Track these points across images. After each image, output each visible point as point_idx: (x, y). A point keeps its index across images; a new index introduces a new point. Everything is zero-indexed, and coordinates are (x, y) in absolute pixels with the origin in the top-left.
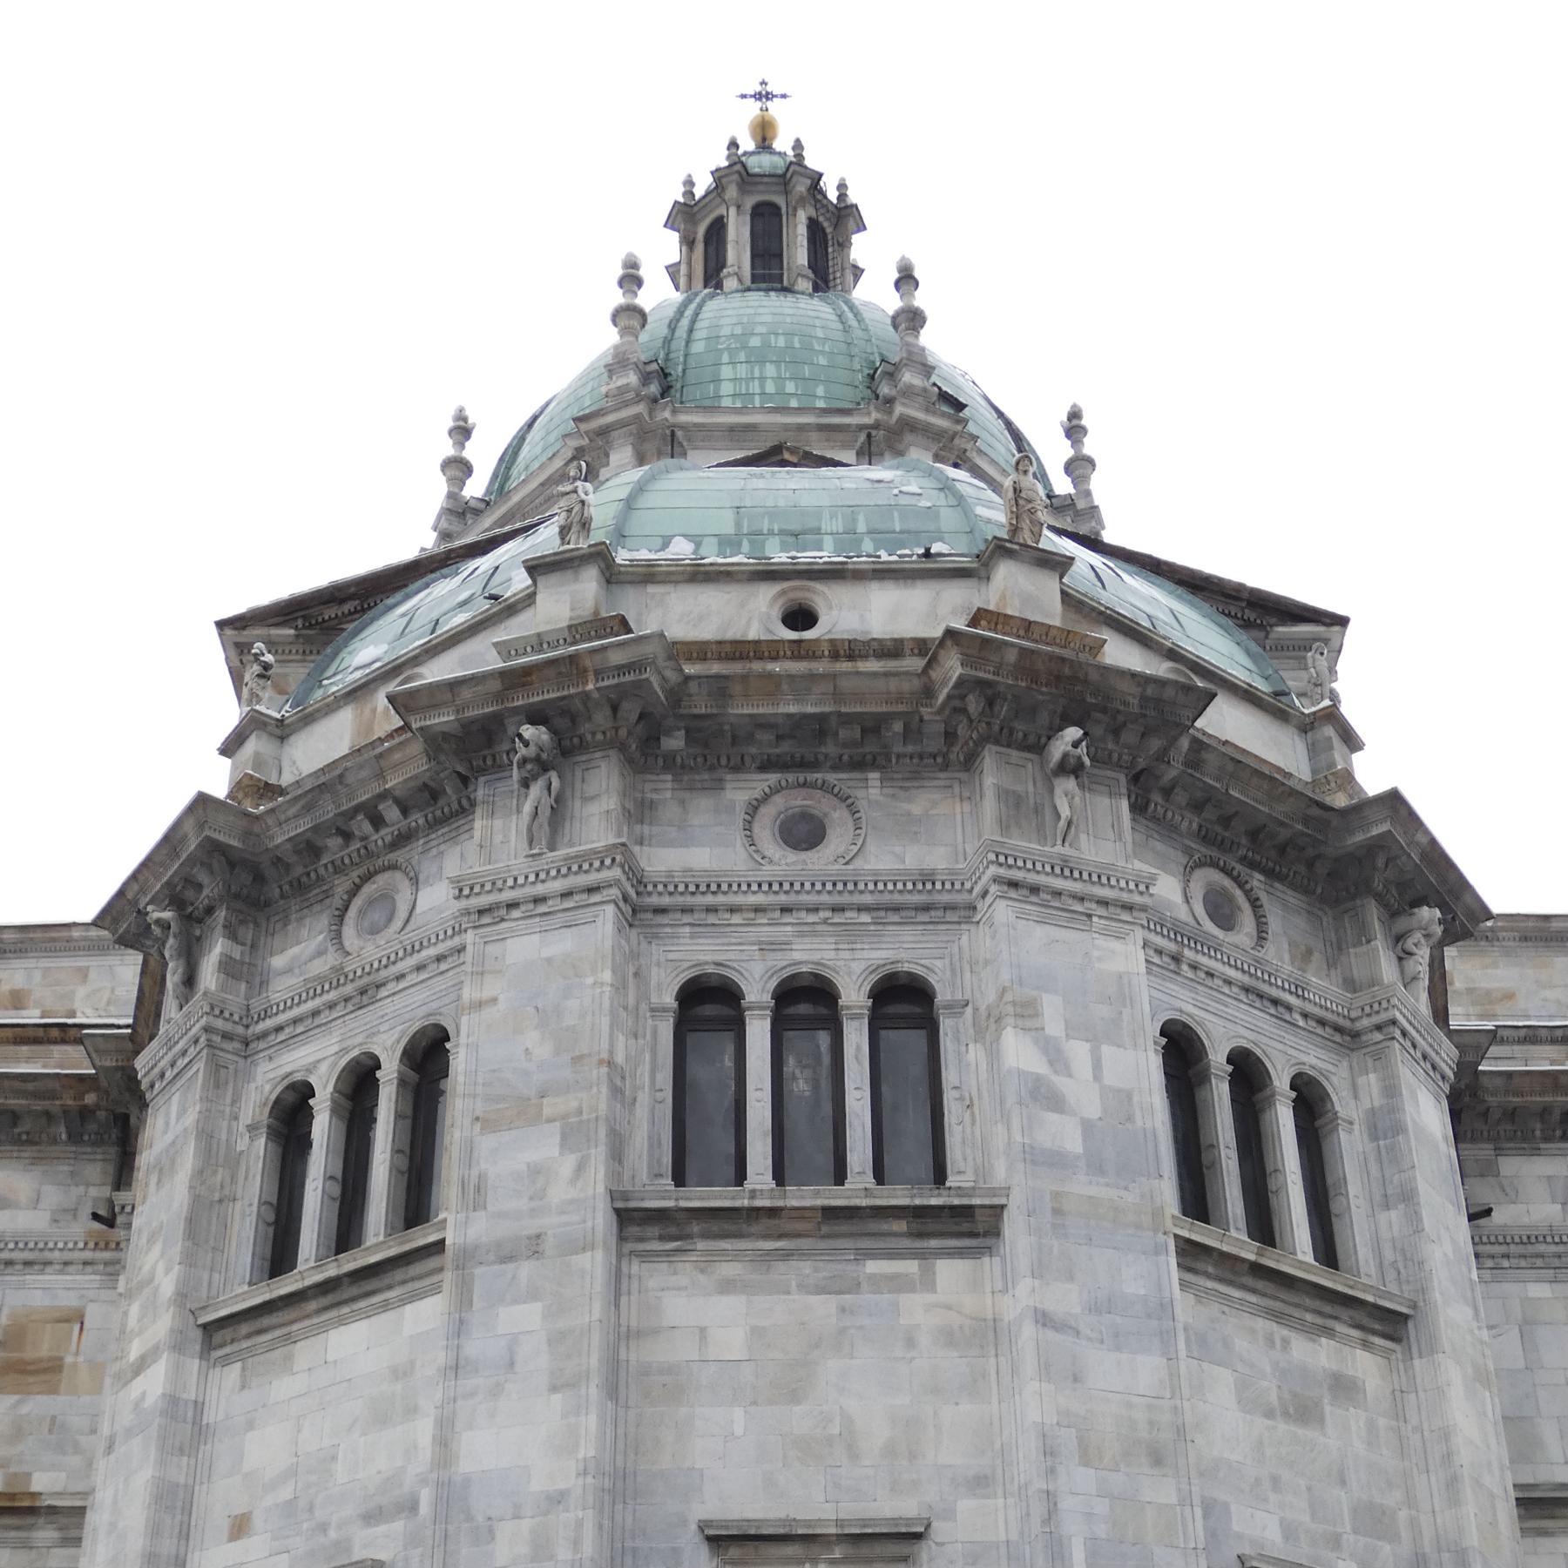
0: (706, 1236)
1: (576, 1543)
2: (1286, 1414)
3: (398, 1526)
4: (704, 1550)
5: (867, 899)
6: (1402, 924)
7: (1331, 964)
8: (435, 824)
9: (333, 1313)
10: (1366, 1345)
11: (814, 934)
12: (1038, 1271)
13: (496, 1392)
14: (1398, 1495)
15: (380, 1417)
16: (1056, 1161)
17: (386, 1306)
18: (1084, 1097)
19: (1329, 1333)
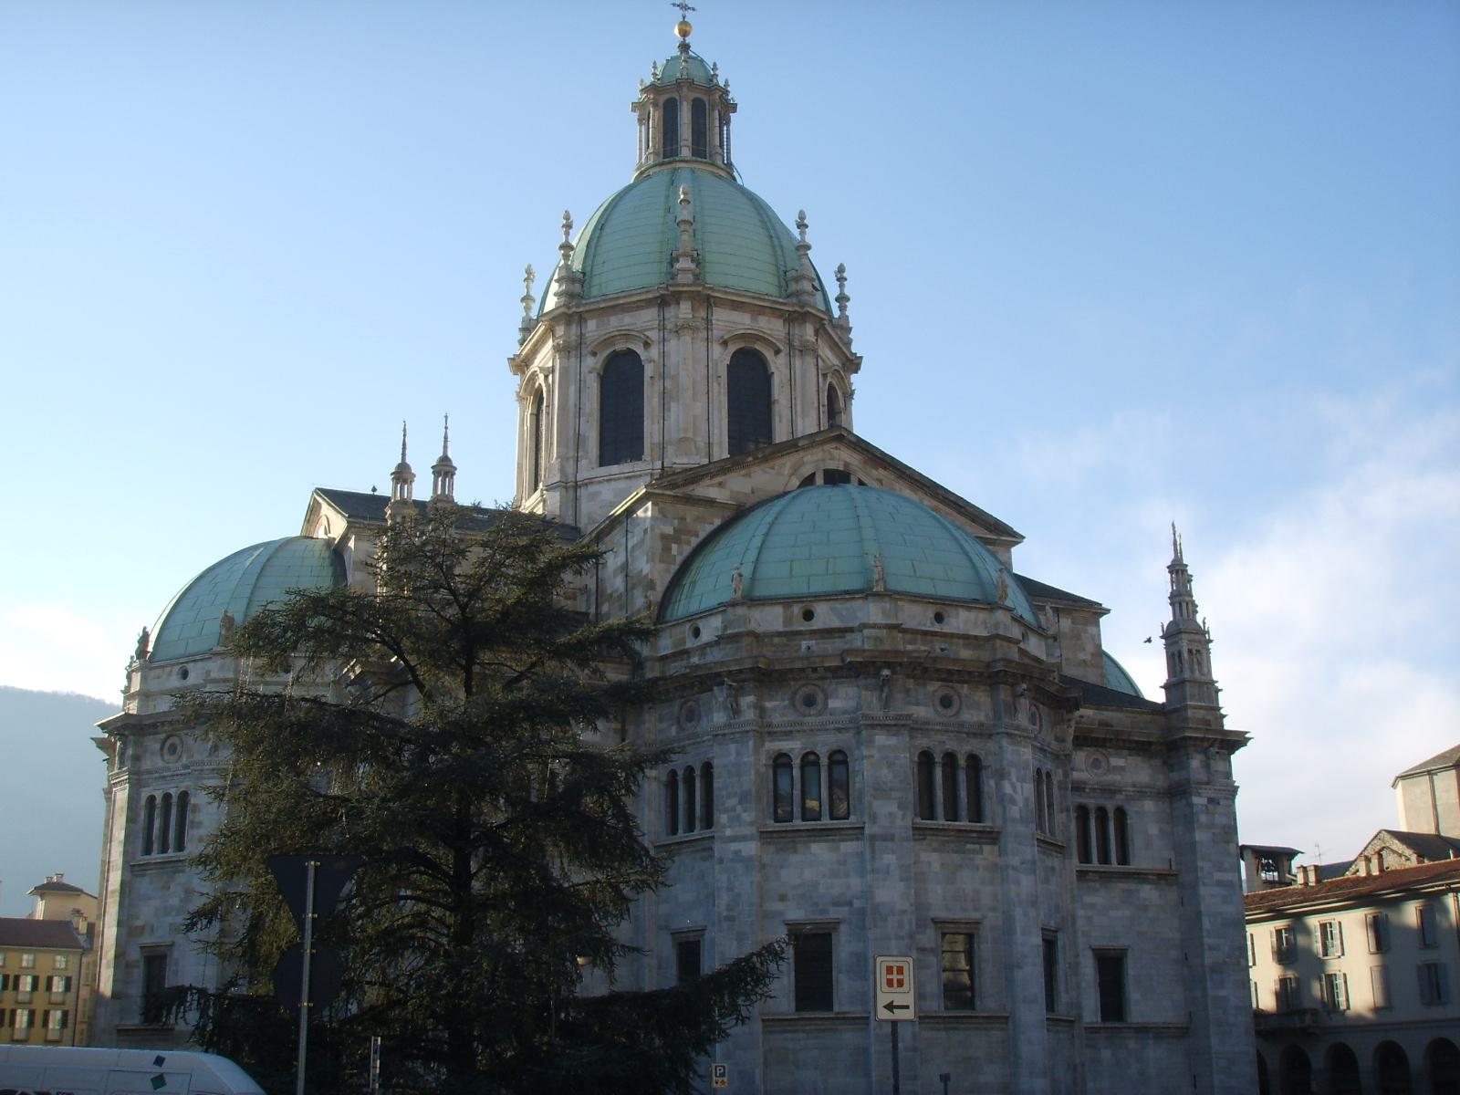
0: (930, 835)
3: (846, 909)
4: (932, 925)
5: (965, 730)
8: (834, 678)
9: (813, 838)
10: (1057, 857)
17: (833, 840)
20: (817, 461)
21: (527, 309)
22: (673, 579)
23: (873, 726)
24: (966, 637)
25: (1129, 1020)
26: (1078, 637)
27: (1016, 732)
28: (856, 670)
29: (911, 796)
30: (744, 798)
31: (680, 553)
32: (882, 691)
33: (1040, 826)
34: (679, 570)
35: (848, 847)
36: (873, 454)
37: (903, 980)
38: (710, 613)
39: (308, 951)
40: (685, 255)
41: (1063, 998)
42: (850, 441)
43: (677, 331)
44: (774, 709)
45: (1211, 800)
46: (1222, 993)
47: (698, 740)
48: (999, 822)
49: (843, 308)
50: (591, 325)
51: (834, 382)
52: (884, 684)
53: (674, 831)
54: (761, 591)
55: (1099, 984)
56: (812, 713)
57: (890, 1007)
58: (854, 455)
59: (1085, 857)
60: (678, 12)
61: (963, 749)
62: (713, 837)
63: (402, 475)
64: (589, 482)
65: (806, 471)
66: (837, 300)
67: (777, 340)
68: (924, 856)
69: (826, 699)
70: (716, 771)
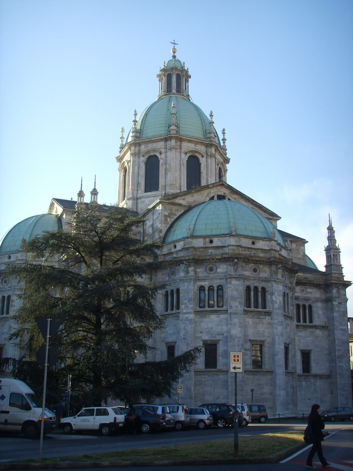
0: (249, 313)
1: (242, 341)
3: (222, 336)
5: (261, 279)
6: (295, 275)
8: (219, 262)
10: (290, 320)
13: (234, 327)
15: (218, 325)
17: (218, 314)
18: (278, 302)
20: (215, 192)
21: (122, 141)
22: (168, 229)
23: (231, 278)
24: (262, 249)
25: (311, 373)
26: (298, 250)
28: (226, 259)
29: (243, 300)
30: (190, 300)
31: (170, 221)
32: (235, 266)
33: (284, 311)
34: (170, 226)
35: (223, 316)
36: (233, 190)
37: (239, 359)
38: (179, 240)
39: (48, 348)
40: (173, 124)
41: (291, 365)
42: (226, 186)
43: (171, 149)
44: (200, 272)
45: (339, 303)
46: (341, 364)
47: (176, 281)
48: (271, 309)
49: (224, 143)
50: (143, 147)
51: (221, 167)
52: (235, 264)
53: (167, 310)
54: (196, 234)
55: (302, 361)
56: (212, 273)
57: (234, 368)
58: (227, 190)
59: (299, 321)
60: (172, 45)
61: (260, 285)
62: (179, 313)
63: (81, 194)
64: (141, 198)
65: (211, 195)
66: (222, 140)
67: (203, 153)
68: (247, 320)
69: (217, 268)
70: (181, 291)
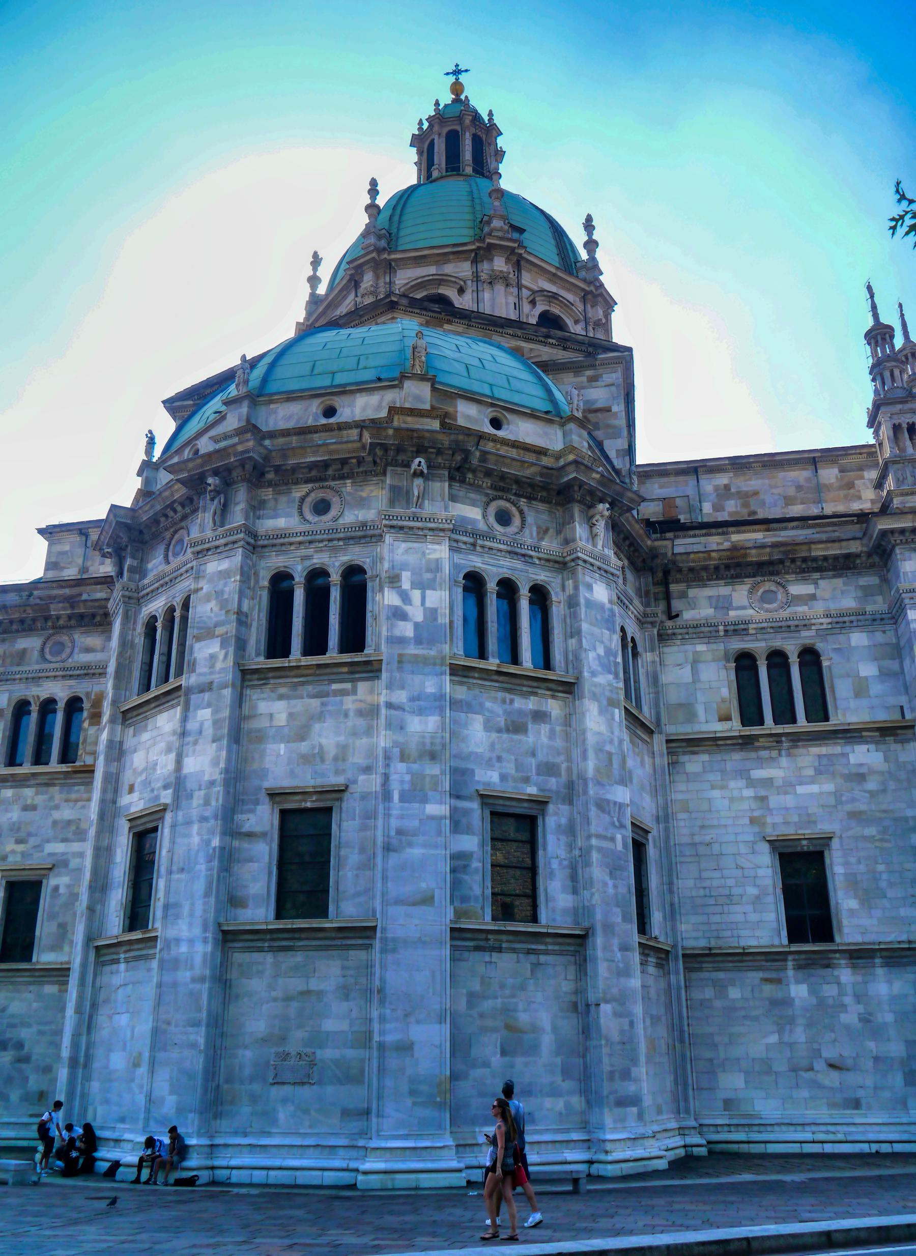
0: (274, 678)
1: (217, 800)
2: (508, 731)
4: (267, 799)
5: (342, 535)
6: (591, 512)
7: (559, 532)
10: (553, 697)
11: (321, 551)
12: (389, 687)
13: (196, 743)
14: (562, 758)
16: (401, 641)
19: (535, 694)
25: (838, 939)
26: (850, 485)
27: (412, 524)
51: (556, 310)
